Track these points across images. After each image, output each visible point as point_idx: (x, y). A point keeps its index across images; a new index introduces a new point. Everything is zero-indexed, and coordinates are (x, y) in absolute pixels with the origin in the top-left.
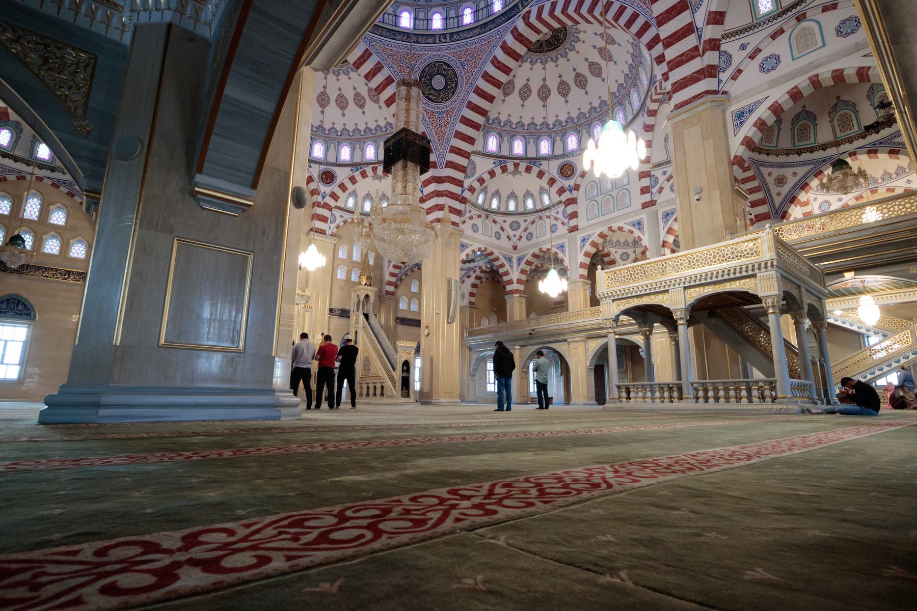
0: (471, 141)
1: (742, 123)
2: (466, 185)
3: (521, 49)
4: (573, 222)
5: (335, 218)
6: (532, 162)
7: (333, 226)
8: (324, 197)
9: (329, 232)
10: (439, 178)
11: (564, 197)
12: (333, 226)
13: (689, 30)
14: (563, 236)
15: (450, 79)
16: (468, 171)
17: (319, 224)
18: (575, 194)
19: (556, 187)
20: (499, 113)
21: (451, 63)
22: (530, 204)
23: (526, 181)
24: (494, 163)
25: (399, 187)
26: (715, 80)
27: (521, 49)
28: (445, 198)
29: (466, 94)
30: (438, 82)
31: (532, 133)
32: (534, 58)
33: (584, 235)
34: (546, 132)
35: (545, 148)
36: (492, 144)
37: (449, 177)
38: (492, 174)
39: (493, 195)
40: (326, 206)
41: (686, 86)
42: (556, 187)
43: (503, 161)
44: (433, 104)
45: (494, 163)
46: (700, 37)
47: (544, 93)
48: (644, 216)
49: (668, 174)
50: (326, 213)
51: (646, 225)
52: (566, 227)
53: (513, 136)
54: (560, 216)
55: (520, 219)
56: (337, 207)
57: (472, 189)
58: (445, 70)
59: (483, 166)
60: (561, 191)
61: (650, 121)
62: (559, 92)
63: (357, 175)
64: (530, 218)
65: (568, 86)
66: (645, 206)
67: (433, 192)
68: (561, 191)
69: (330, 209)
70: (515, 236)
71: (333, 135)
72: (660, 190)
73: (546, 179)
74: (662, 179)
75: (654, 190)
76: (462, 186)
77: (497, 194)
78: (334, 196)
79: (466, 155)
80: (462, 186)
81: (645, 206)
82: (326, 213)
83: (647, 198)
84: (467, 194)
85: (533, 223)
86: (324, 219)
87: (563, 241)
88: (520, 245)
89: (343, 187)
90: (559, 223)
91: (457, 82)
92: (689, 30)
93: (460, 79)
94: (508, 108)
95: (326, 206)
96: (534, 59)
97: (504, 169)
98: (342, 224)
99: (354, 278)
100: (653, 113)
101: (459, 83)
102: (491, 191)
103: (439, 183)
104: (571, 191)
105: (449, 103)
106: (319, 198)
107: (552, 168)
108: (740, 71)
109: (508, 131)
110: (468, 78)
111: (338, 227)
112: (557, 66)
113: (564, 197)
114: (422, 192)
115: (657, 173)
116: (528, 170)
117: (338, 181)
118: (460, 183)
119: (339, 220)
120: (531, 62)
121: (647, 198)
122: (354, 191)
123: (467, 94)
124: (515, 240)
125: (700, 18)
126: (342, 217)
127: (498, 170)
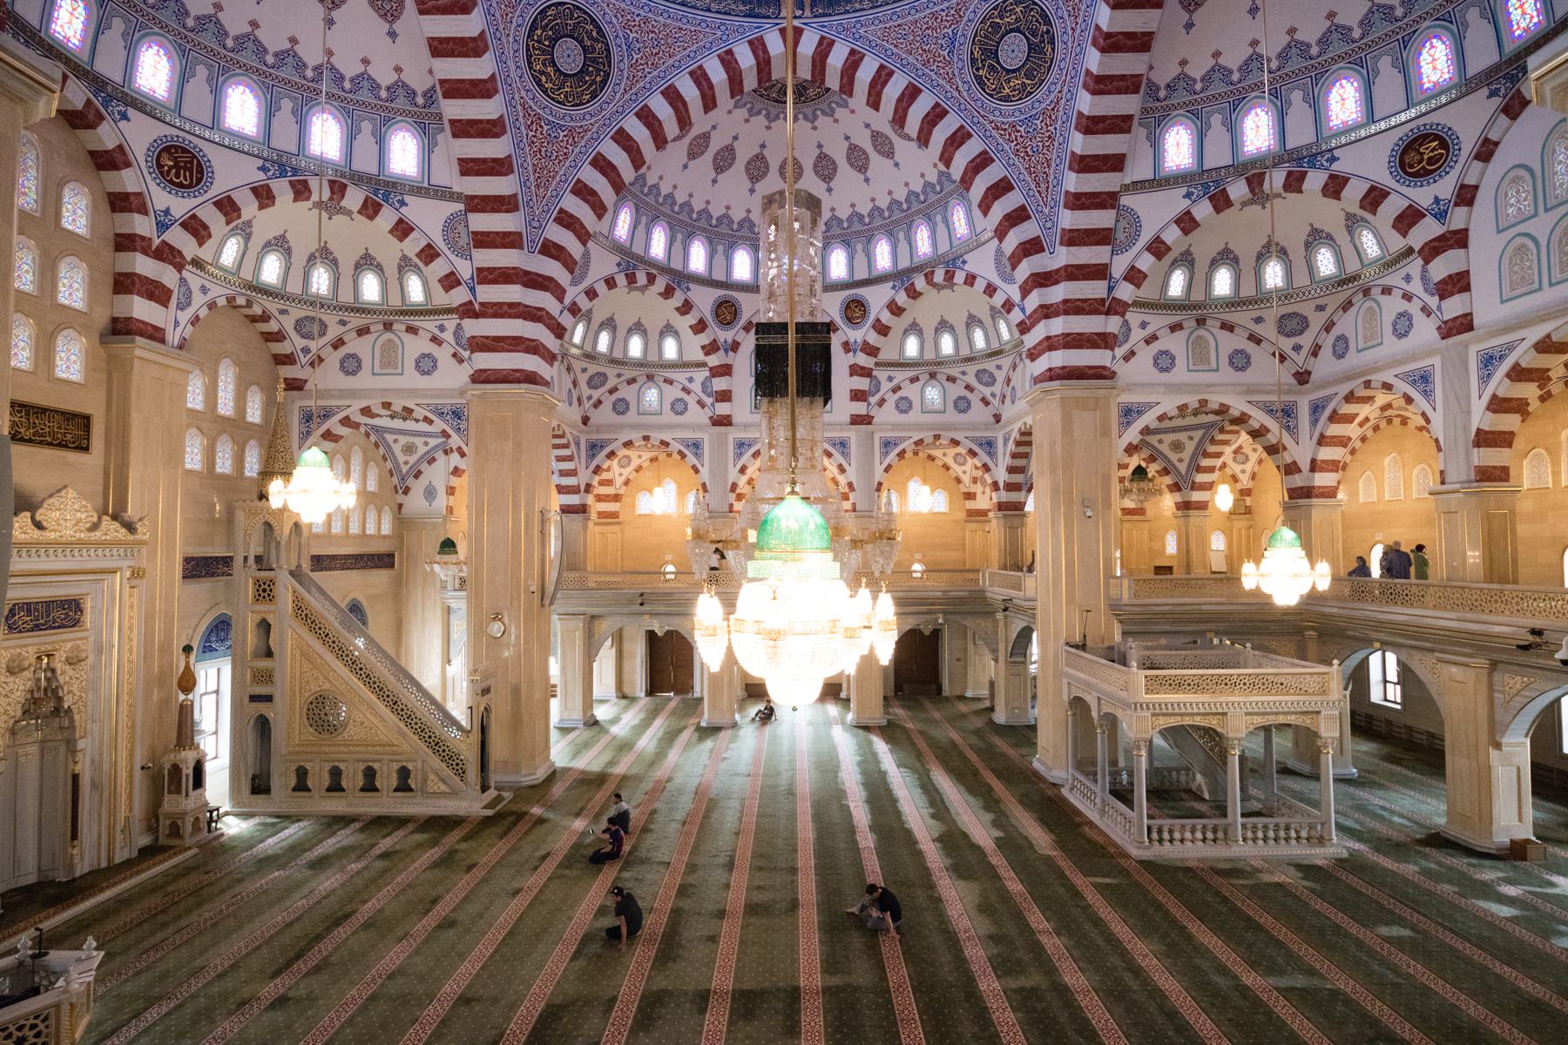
0: (599, 209)
1: (1129, 424)
2: (567, 300)
3: (750, 82)
4: (723, 409)
5: (188, 295)
6: (677, 279)
7: (185, 316)
8: (162, 227)
9: (173, 337)
10: (527, 273)
11: (713, 360)
12: (185, 316)
13: (1099, 272)
14: (700, 427)
15: (594, 60)
16: (577, 271)
17: (142, 309)
18: (730, 358)
19: (704, 339)
20: (661, 178)
21: (606, 28)
22: (635, 347)
23: (653, 306)
24: (619, 265)
25: (782, 434)
26: (1108, 353)
27: (750, 82)
28: (540, 326)
29: (615, 107)
30: (569, 56)
31: (685, 223)
32: (758, 106)
33: (742, 435)
34: (704, 230)
35: (698, 259)
36: (623, 224)
37: (551, 279)
38: (610, 283)
39: (602, 326)
40: (167, 254)
41: (1081, 347)
42: (704, 339)
43: (634, 266)
44: (544, 100)
45: (619, 265)
46: (1111, 289)
47: (724, 160)
48: (853, 435)
49: (895, 382)
50: (167, 275)
51: (853, 449)
52: (708, 412)
53: (654, 220)
54: (696, 387)
55: (611, 372)
56: (197, 263)
57: (574, 310)
58: (589, 34)
59: (603, 264)
60: (711, 348)
61: (902, 299)
62: (747, 169)
63: (281, 188)
64: (629, 373)
65: (767, 167)
66: (857, 420)
67: (511, 305)
68: (711, 348)
69: (179, 268)
70: (590, 398)
71: (208, 39)
72: (882, 402)
73: (691, 319)
74: (886, 386)
75: (873, 400)
76: (561, 302)
77: (610, 324)
78: (197, 228)
79: (583, 236)
80: (561, 302)
81: (857, 420)
82: (167, 275)
83: (860, 408)
84: (566, 320)
85: (631, 381)
86: (158, 293)
87: (698, 435)
88: (597, 417)
89: (227, 207)
90: (691, 401)
91: (607, 75)
92: (1099, 272)
93: (615, 72)
94: (670, 170)
95: (167, 254)
96: (758, 106)
97: (631, 279)
98: (203, 313)
99: (224, 465)
100: (914, 294)
101: (613, 79)
102: (599, 317)
103: (526, 285)
104: (726, 351)
105: (577, 112)
106: (142, 225)
107: (705, 299)
108: (1133, 353)
109: (653, 208)
110: (633, 81)
111: (195, 321)
112: (768, 128)
113: (713, 360)
114: (472, 290)
115: (881, 375)
116: (668, 293)
117: (217, 189)
118: (559, 293)
119: (198, 300)
120: (750, 110)
121: (860, 408)
122: (249, 224)
123: (621, 112)
124: (587, 405)
125: (1119, 267)
126: (204, 290)
127: (621, 280)
